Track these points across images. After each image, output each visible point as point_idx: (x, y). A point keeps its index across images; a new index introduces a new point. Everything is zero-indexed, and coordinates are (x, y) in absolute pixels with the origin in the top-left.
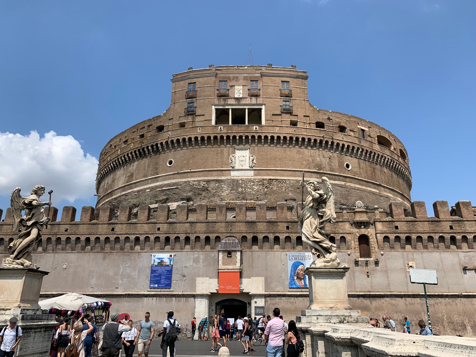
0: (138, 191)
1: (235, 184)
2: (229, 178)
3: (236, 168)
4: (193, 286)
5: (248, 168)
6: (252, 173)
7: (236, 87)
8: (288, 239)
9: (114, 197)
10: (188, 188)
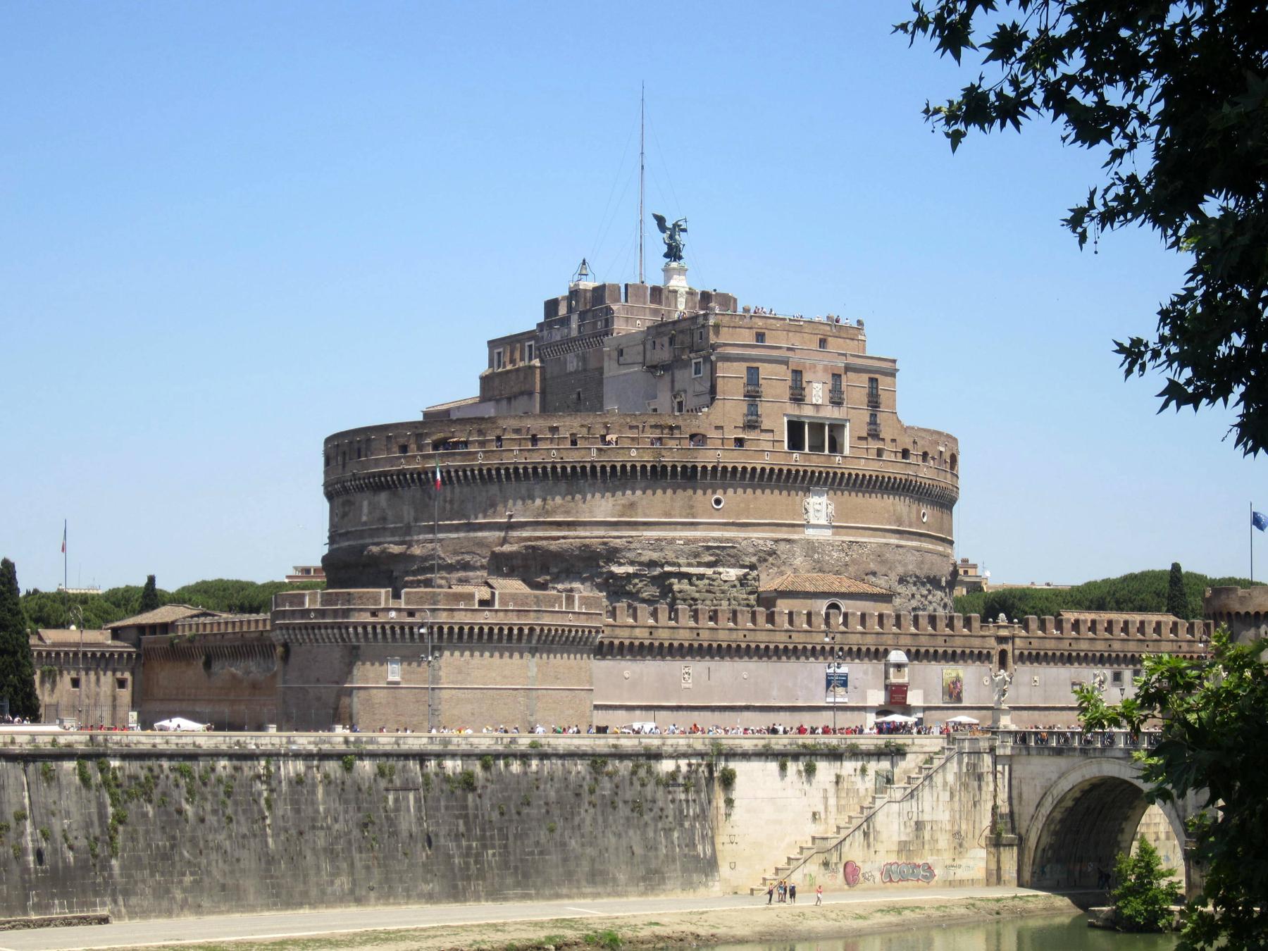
0: (657, 540)
1: (811, 548)
2: (802, 536)
3: (812, 522)
4: (865, 698)
5: (823, 522)
6: (829, 532)
7: (815, 385)
8: (945, 652)
9: (583, 534)
10: (751, 550)
